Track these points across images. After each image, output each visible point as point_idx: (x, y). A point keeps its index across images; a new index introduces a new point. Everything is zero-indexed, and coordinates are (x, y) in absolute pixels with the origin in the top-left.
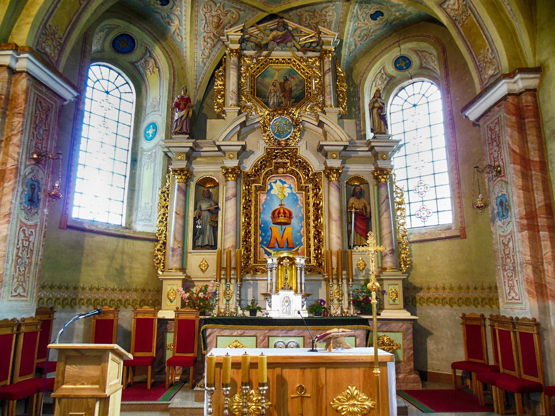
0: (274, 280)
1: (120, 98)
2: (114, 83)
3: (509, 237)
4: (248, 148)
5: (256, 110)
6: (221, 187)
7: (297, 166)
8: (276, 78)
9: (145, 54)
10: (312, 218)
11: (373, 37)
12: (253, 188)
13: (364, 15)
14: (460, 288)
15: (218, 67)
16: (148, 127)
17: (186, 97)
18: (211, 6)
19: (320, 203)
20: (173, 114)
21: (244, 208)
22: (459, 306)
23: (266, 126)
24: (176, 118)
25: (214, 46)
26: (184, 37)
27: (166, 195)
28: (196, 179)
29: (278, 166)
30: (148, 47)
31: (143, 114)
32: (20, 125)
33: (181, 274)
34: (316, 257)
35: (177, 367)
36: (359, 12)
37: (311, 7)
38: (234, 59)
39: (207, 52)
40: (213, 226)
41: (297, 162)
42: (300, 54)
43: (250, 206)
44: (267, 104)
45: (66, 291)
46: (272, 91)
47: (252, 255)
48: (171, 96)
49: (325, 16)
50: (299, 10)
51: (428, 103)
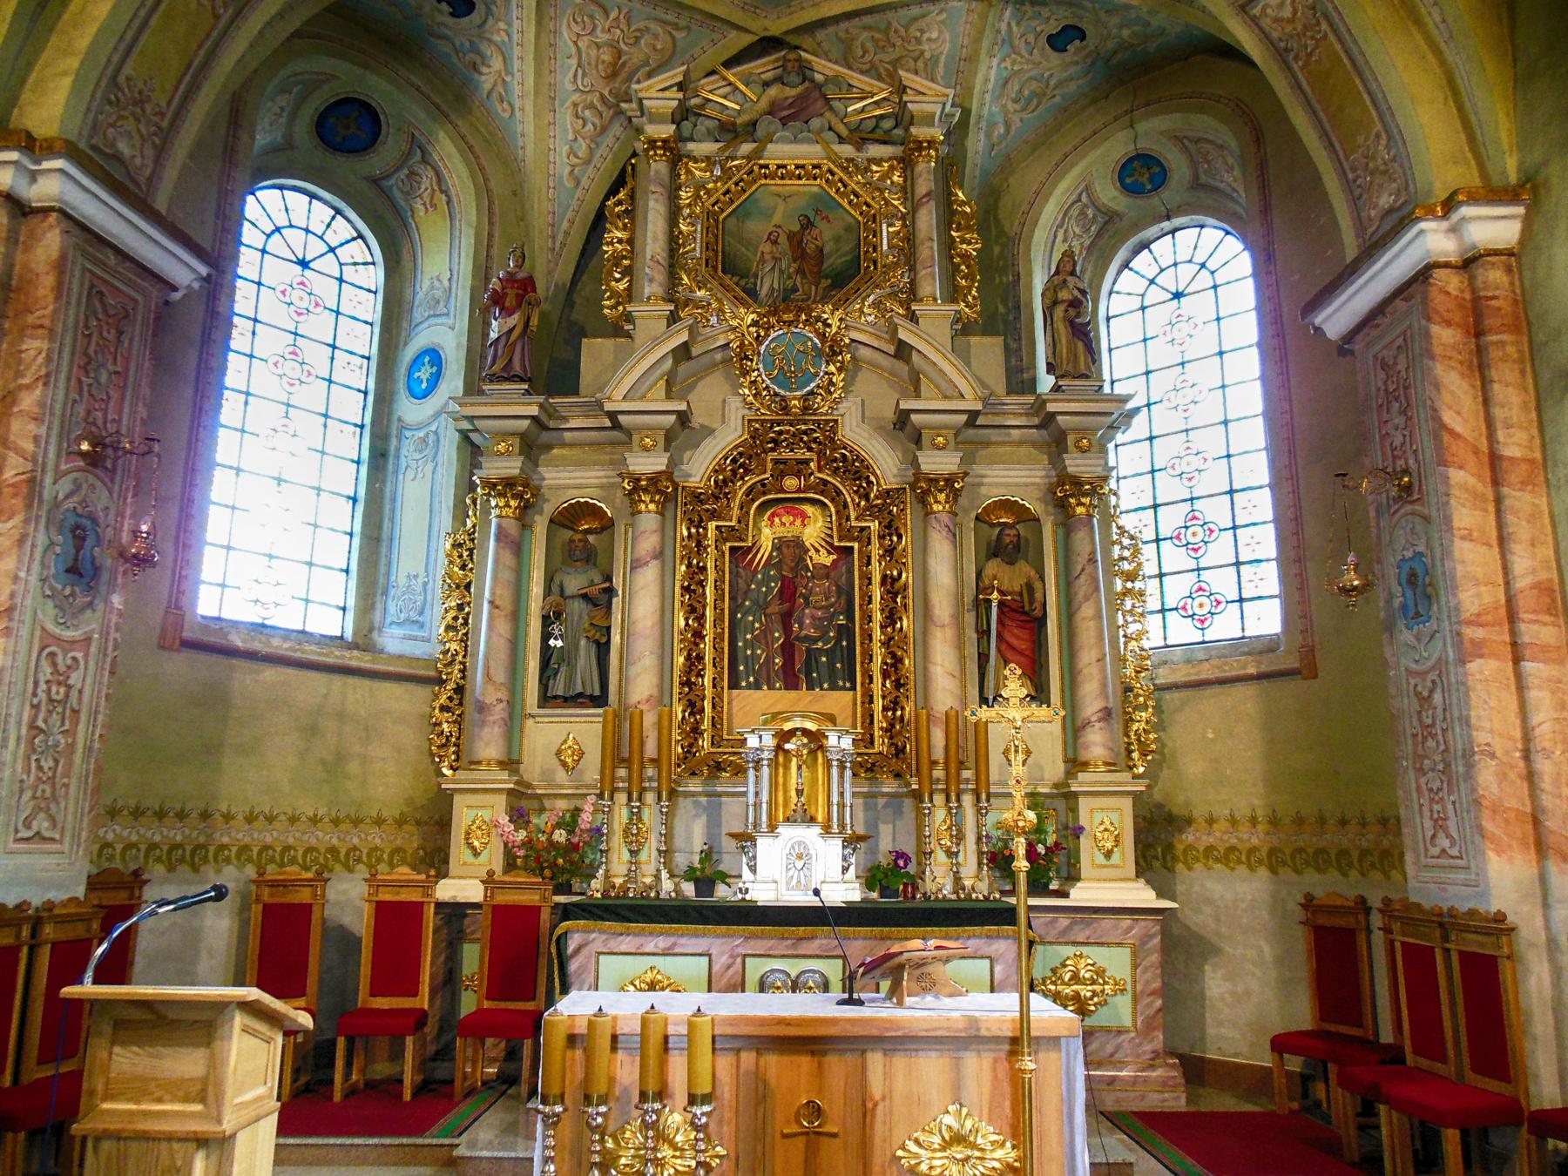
0: (765, 797)
1: (341, 280)
2: (321, 238)
3: (1433, 676)
4: (697, 420)
5: (721, 311)
6: (620, 529)
7: (835, 471)
8: (777, 218)
9: (410, 153)
10: (878, 617)
11: (1058, 99)
12: (711, 533)
13: (1031, 38)
14: (1299, 820)
15: (613, 191)
16: (417, 360)
17: (521, 275)
18: (592, 17)
19: (900, 575)
20: (487, 325)
21: (686, 589)
22: (1297, 871)
23: (747, 358)
24: (493, 335)
25: (604, 129)
26: (517, 104)
27: (465, 554)
28: (549, 509)
30: (417, 134)
31: (405, 325)
32: (40, 359)
33: (504, 775)
34: (889, 730)
35: (489, 1041)
36: (1015, 29)
37: (877, 17)
38: (659, 167)
39: (582, 147)
40: (597, 643)
41: (835, 460)
42: (847, 150)
43: (701, 584)
44: (752, 293)
45: (179, 825)
46: (767, 257)
47: (706, 725)
48: (482, 272)
49: (918, 41)
50: (844, 25)
51: (1215, 287)
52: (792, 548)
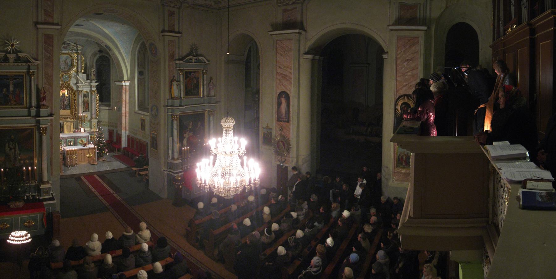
8: (63, 59)
29: (63, 87)
42: (71, 52)
52: (64, 94)
